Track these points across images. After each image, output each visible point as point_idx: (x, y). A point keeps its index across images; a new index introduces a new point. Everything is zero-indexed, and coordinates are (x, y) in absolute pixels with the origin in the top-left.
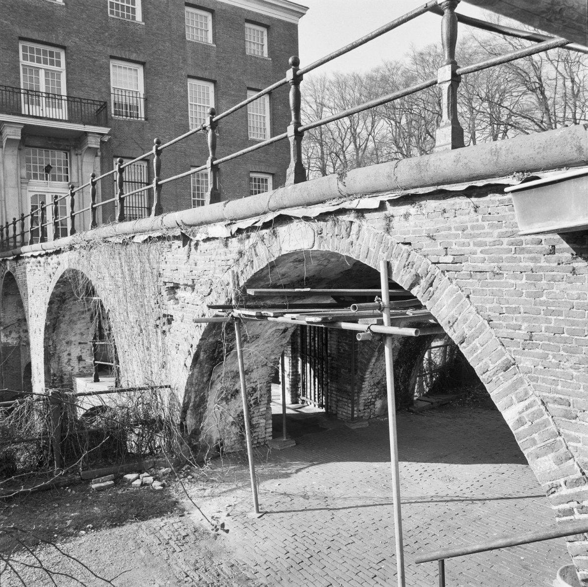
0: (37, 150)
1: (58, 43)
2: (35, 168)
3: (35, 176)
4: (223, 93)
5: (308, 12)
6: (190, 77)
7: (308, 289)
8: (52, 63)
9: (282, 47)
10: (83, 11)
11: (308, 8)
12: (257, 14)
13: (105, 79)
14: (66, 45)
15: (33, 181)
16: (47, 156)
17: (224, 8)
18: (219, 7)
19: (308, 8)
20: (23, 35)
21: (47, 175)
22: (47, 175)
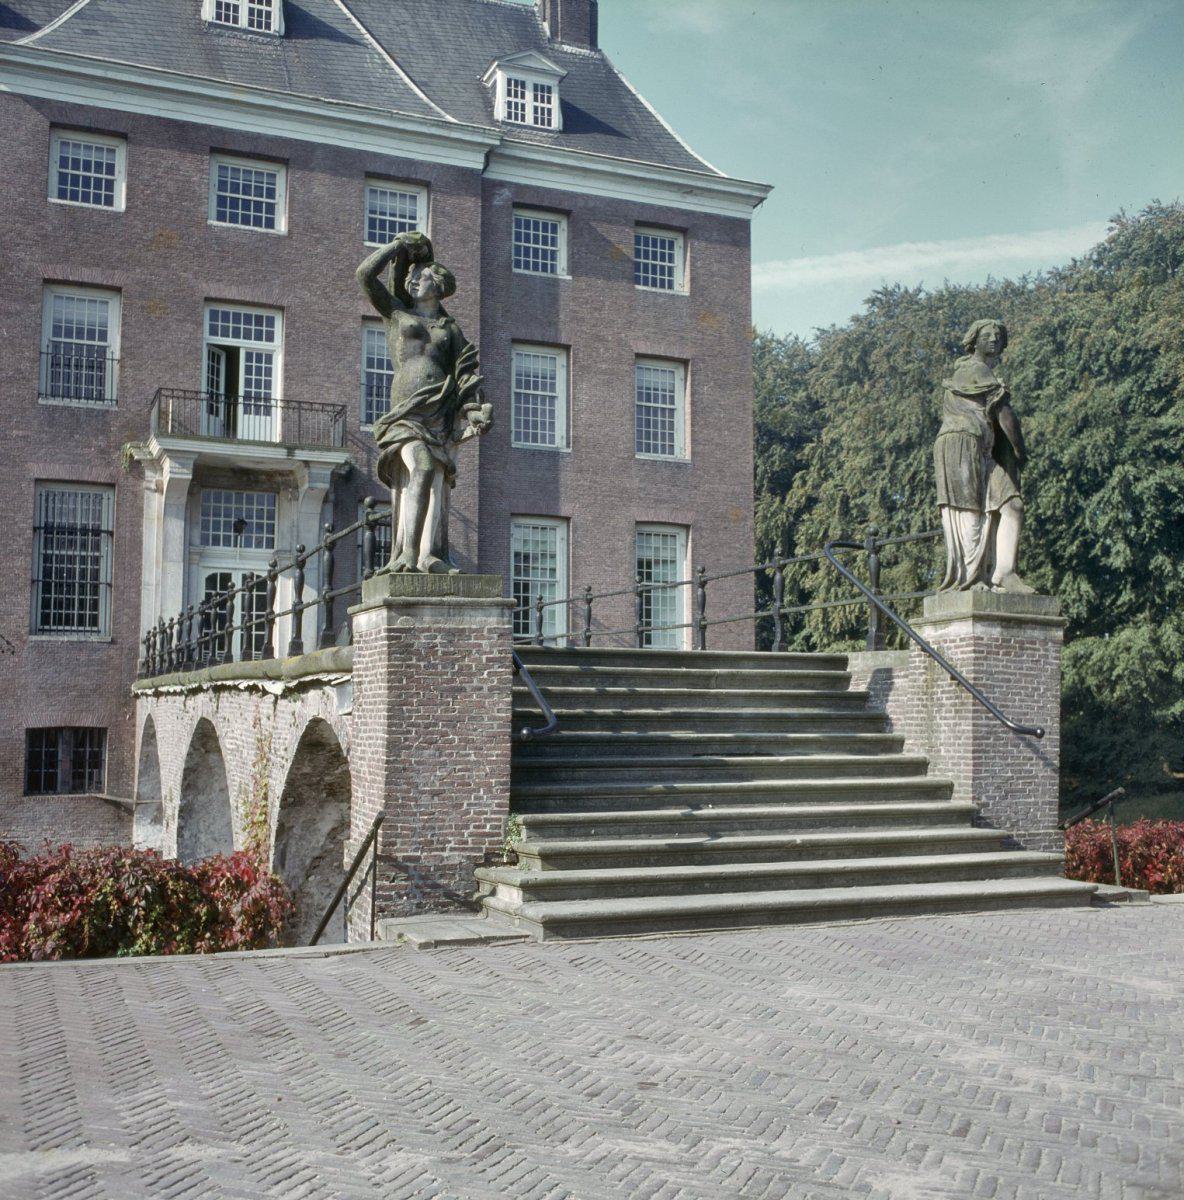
0: (223, 492)
1: (270, 302)
3: (216, 542)
5: (771, 195)
6: (516, 341)
7: (609, 733)
8: (259, 337)
9: (715, 268)
10: (317, 240)
11: (768, 188)
12: (661, 208)
13: (350, 359)
14: (285, 303)
15: (211, 549)
16: (239, 501)
17: (591, 204)
18: (581, 204)
19: (768, 188)
20: (213, 294)
21: (236, 538)
22: (236, 538)
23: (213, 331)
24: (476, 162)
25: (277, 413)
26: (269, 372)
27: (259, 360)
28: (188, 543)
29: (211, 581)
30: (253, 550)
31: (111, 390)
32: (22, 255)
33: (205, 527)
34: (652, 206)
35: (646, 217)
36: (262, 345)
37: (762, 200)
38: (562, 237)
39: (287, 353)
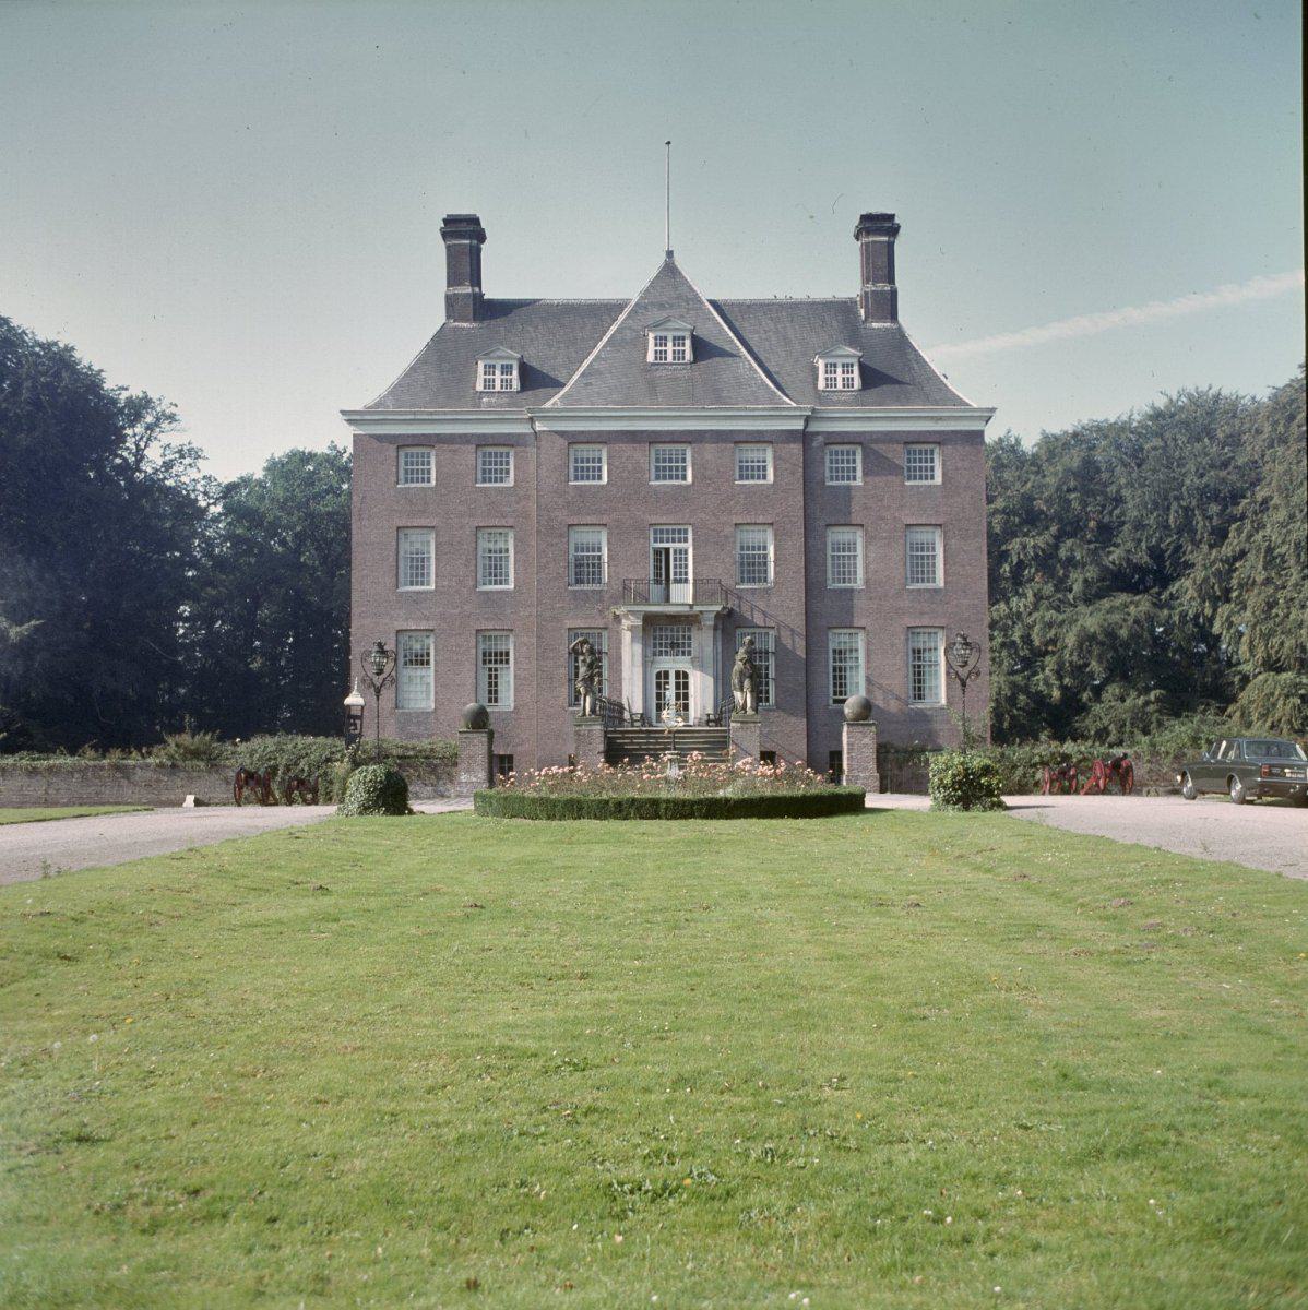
2: (661, 644)
3: (661, 654)
4: (873, 538)
5: (997, 412)
8: (680, 541)
11: (993, 410)
15: (658, 658)
17: (874, 437)
19: (993, 410)
23: (656, 541)
24: (799, 425)
25: (690, 586)
26: (686, 559)
27: (681, 553)
28: (645, 656)
29: (658, 675)
30: (680, 657)
31: (605, 578)
32: (557, 514)
33: (655, 647)
34: (915, 432)
35: (910, 440)
36: (682, 545)
37: (990, 418)
38: (859, 458)
39: (694, 549)
